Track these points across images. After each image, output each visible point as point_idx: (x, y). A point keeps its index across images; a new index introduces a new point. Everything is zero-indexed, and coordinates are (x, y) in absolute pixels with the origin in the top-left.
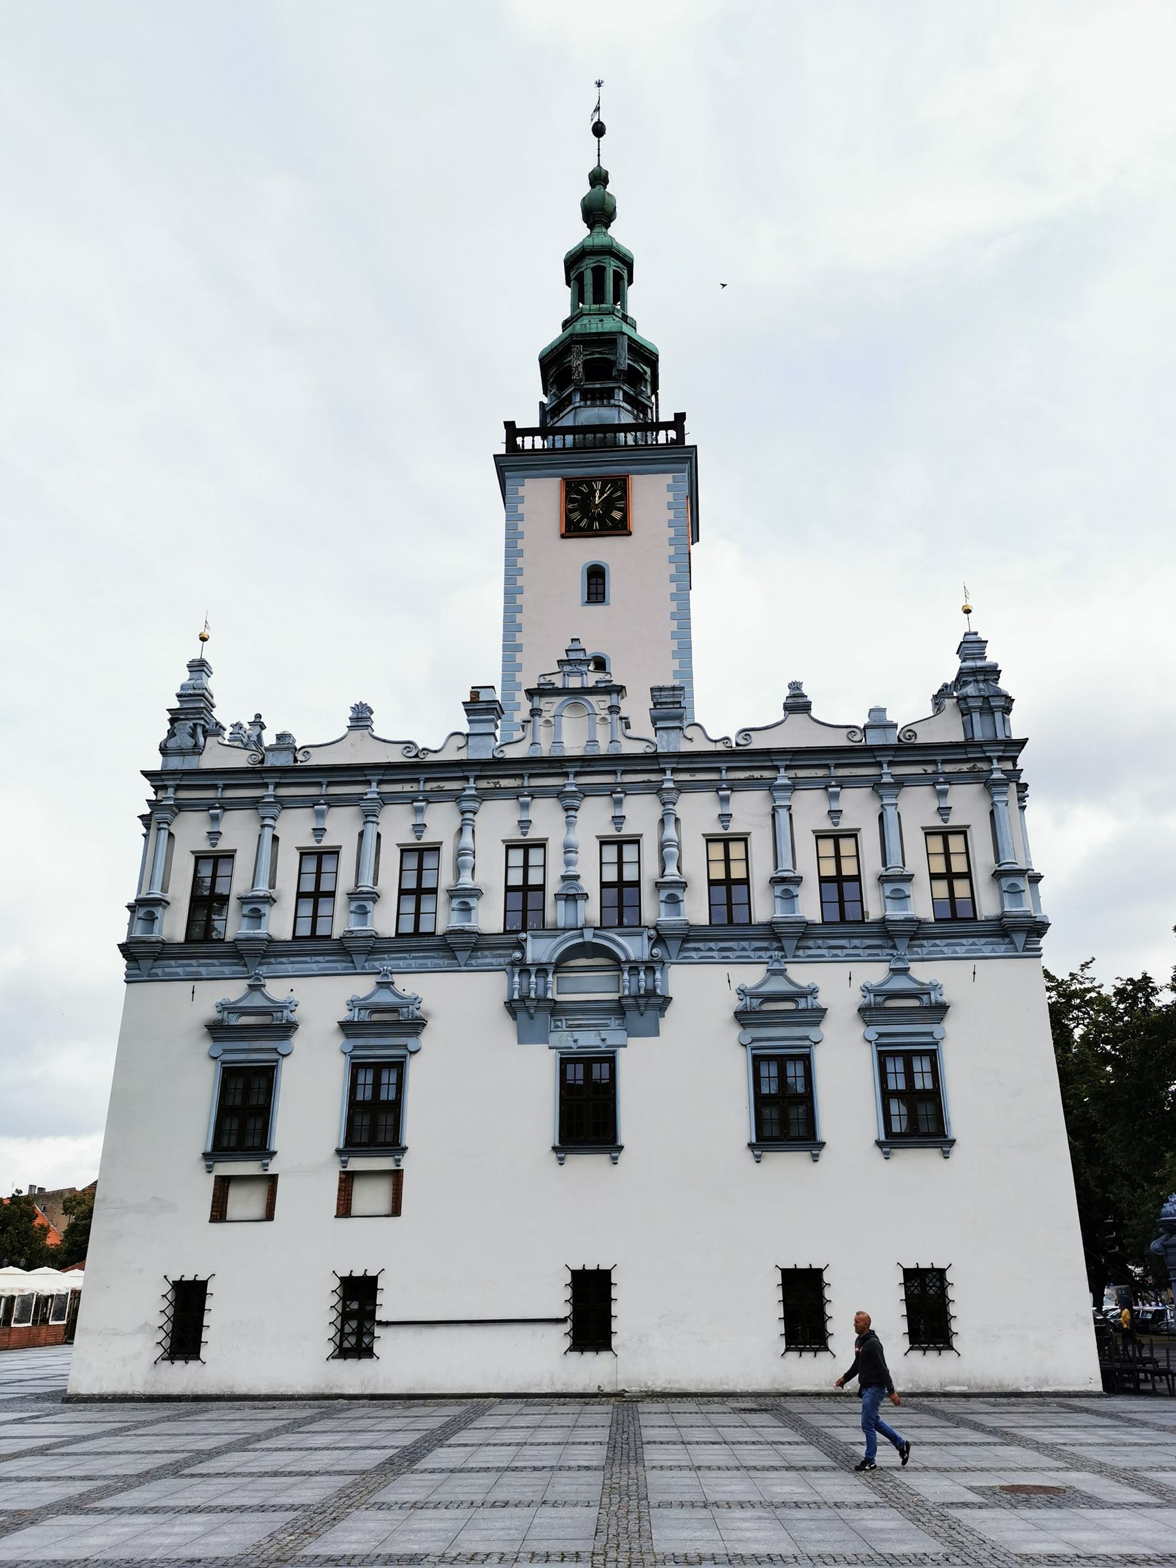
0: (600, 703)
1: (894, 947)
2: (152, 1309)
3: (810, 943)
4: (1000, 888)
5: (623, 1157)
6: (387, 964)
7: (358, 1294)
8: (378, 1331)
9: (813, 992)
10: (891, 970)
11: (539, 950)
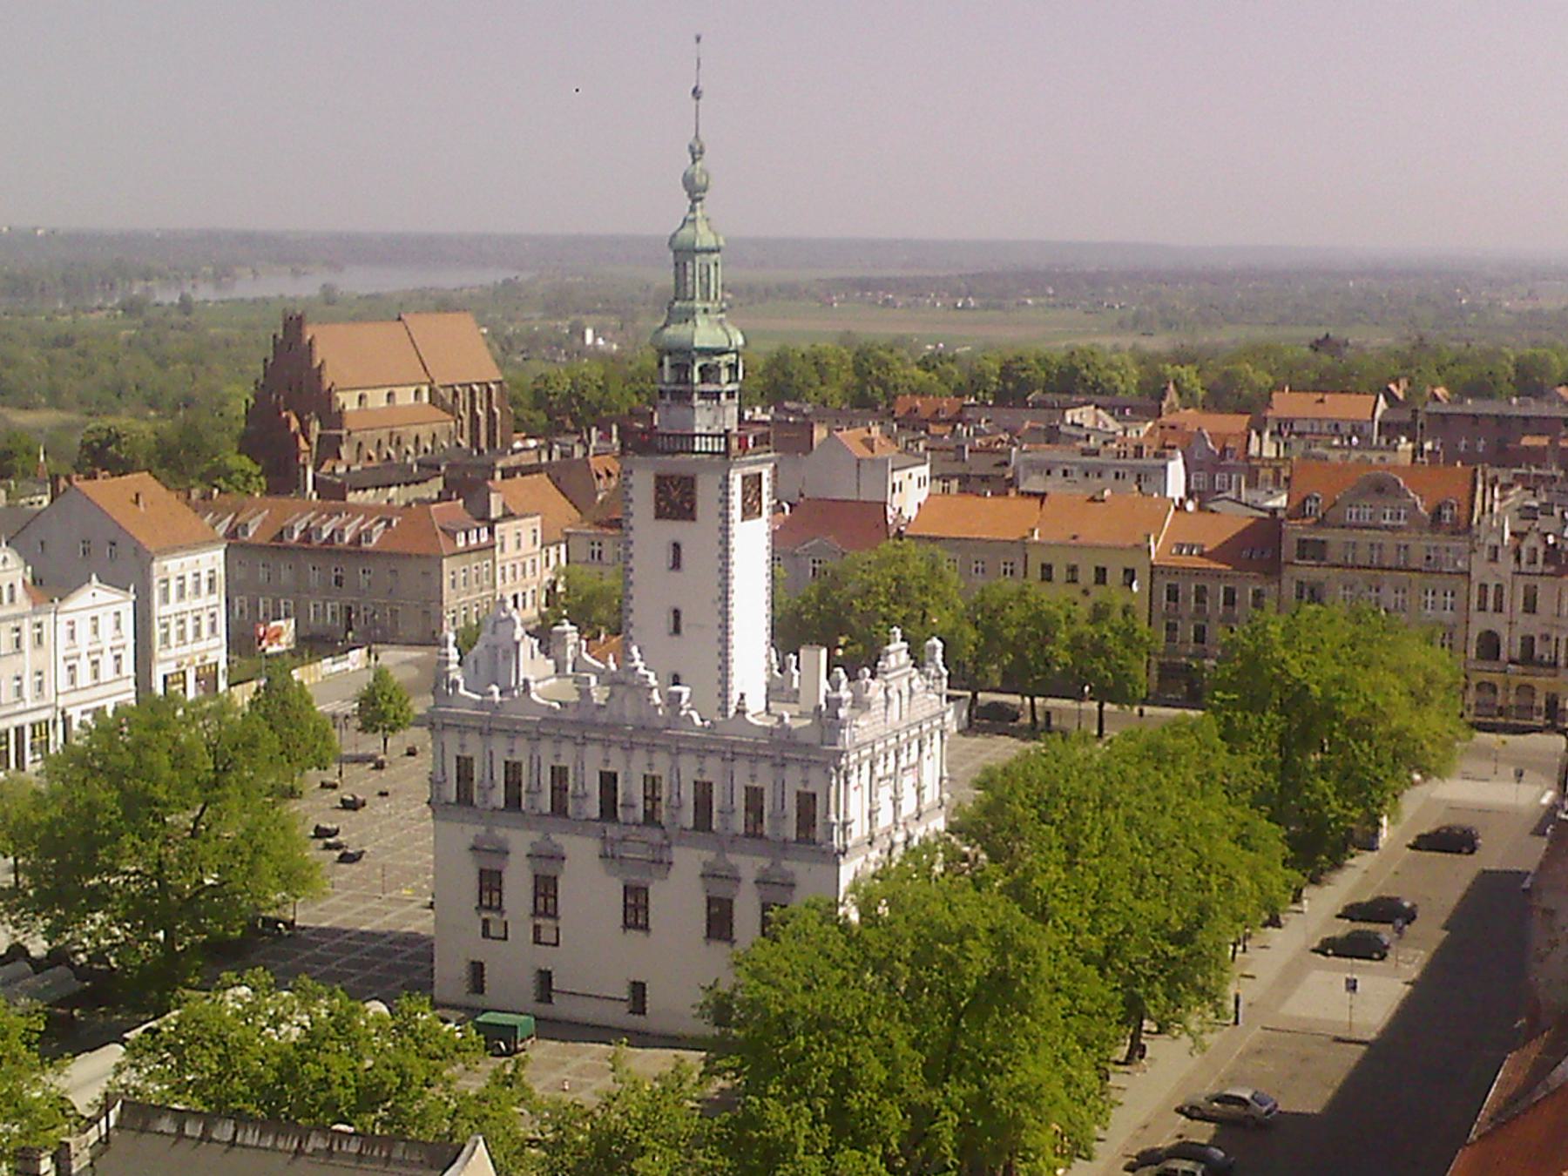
2: (462, 971)
7: (545, 978)
11: (612, 831)
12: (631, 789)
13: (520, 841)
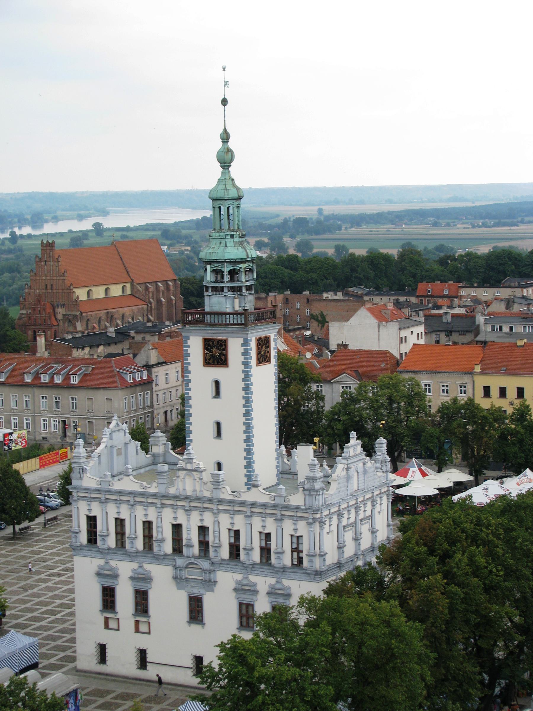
0: (196, 475)
2: (93, 651)
3: (255, 569)
5: (206, 626)
6: (141, 559)
7: (142, 654)
8: (148, 664)
11: (180, 562)
12: (191, 535)
13: (125, 568)
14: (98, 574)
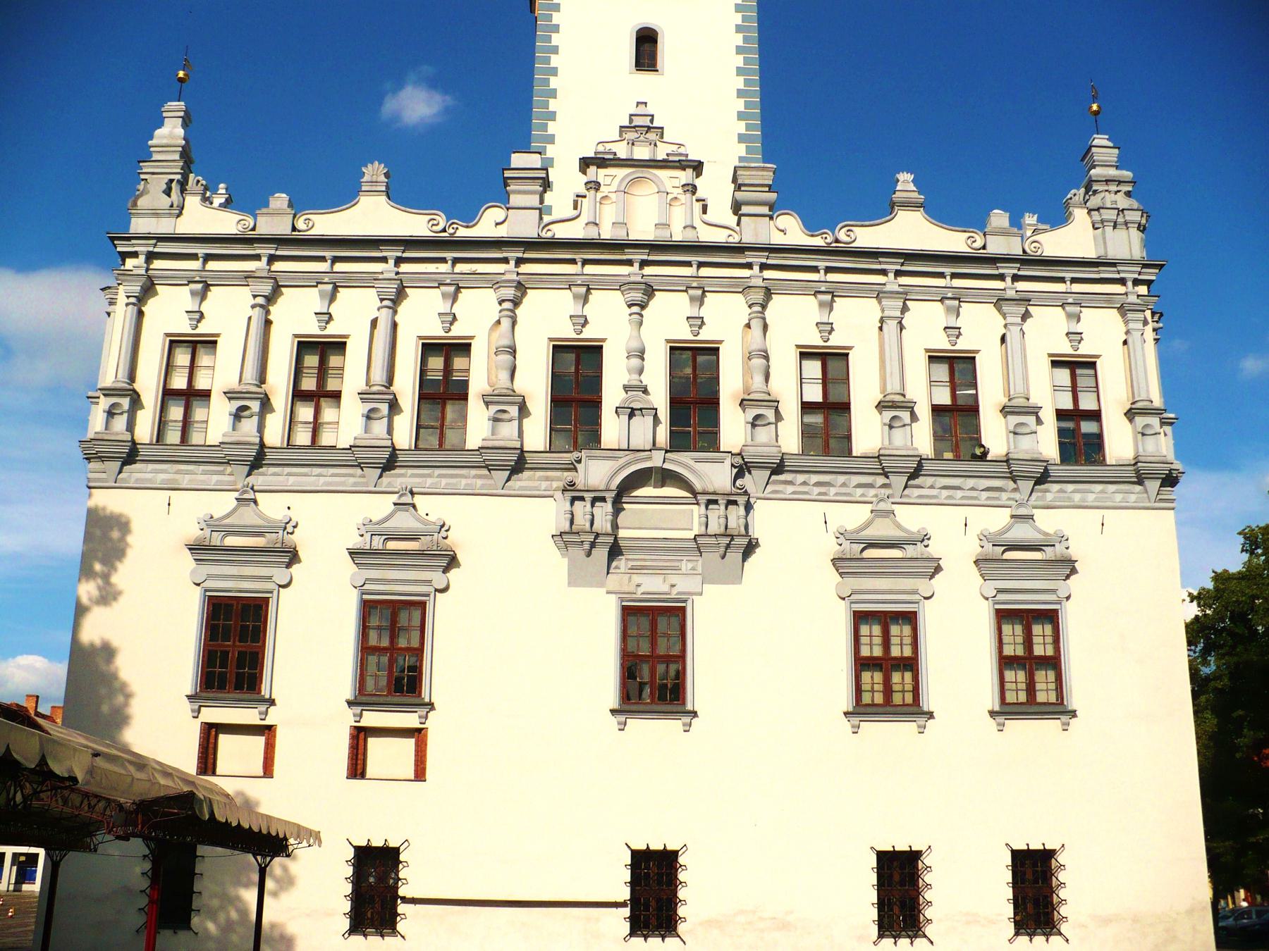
0: (673, 179)
1: (1016, 490)
4: (1134, 428)
8: (402, 908)
9: (924, 539)
10: (1013, 516)
11: (598, 472)
13: (329, 523)
14: (199, 550)
